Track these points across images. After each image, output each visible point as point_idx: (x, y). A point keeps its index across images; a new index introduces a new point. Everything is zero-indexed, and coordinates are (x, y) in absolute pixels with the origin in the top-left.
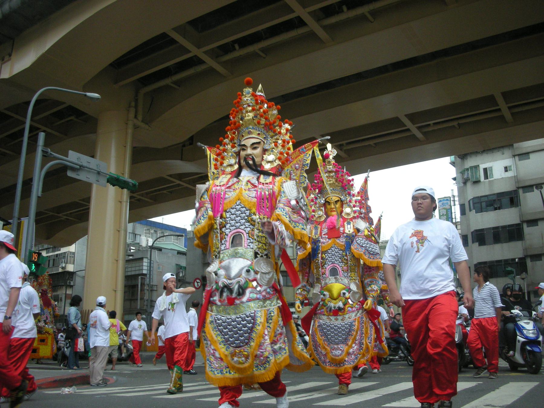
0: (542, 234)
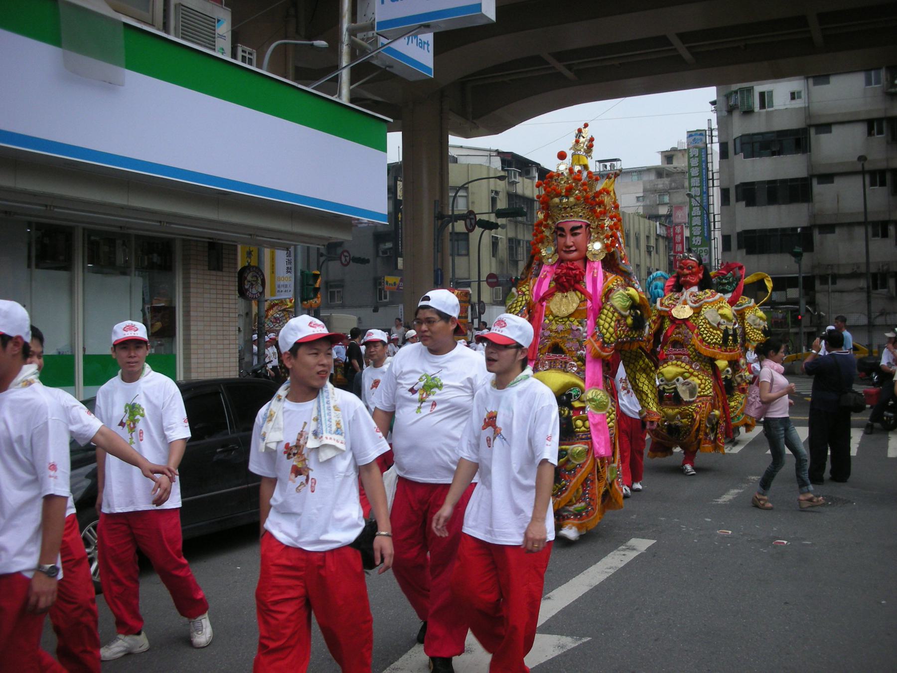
0: (838, 196)
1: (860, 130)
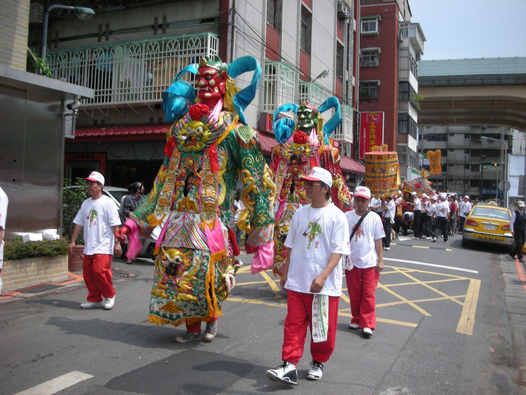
1: (463, 136)
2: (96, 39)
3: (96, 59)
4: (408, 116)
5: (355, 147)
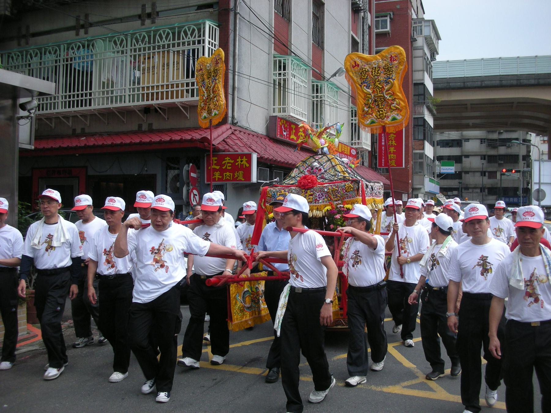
1: (479, 141)
2: (73, 33)
3: (73, 56)
4: (425, 120)
5: (372, 155)
